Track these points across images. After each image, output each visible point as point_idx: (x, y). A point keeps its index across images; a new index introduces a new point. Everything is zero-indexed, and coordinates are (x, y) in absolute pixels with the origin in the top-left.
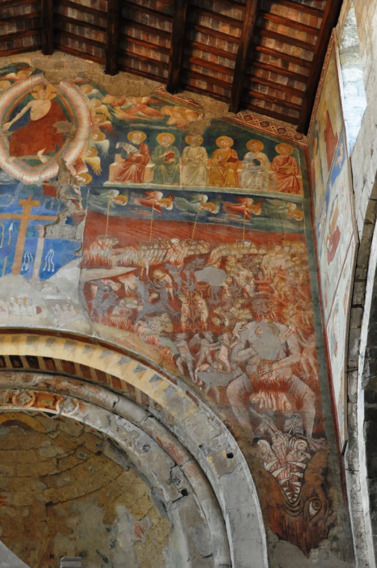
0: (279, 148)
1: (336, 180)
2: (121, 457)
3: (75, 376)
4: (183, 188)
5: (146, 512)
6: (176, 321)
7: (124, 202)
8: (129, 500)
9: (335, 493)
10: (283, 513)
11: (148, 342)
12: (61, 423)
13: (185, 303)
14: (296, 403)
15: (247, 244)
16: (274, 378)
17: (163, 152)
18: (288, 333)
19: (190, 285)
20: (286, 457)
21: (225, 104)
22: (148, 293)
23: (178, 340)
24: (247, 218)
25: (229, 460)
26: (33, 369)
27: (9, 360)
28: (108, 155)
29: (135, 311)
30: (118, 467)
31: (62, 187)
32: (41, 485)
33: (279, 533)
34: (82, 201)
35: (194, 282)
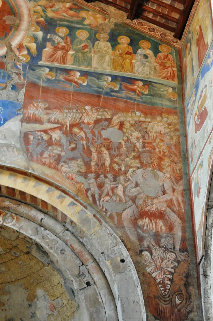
0: (161, 47)
1: (206, 74)
2: (44, 257)
3: (14, 198)
4: (94, 71)
5: (59, 295)
6: (87, 164)
7: (52, 78)
8: (46, 286)
9: (193, 290)
10: (158, 302)
11: (68, 178)
12: (3, 230)
13: (94, 152)
14: (169, 228)
15: (138, 114)
16: (155, 209)
17: (80, 44)
18: (165, 178)
19: (98, 139)
20: (162, 264)
21: (124, 13)
22: (68, 143)
23: (89, 178)
24: (138, 95)
25: (122, 263)
28: (41, 42)
29: (59, 155)
30: (41, 264)
31: (9, 63)
33: (155, 315)
34: (23, 74)
35: (101, 138)
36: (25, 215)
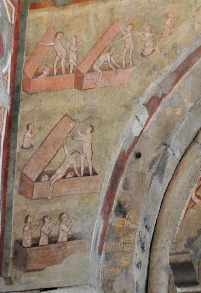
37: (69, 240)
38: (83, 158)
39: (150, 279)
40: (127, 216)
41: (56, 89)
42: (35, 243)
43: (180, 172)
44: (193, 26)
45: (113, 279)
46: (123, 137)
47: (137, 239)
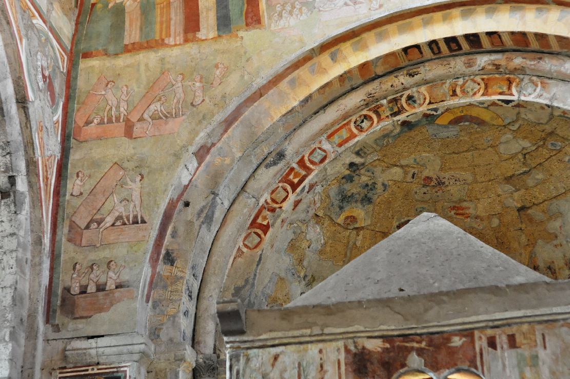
3: (529, 49)
12: (522, 110)
26: (474, 50)
27: (444, 44)
32: (508, 188)
36: (555, 74)
37: (117, 287)
38: (132, 205)
39: (197, 327)
40: (175, 264)
41: (106, 137)
42: (83, 291)
43: (228, 221)
44: (242, 76)
45: (160, 327)
46: (172, 185)
47: (184, 287)
